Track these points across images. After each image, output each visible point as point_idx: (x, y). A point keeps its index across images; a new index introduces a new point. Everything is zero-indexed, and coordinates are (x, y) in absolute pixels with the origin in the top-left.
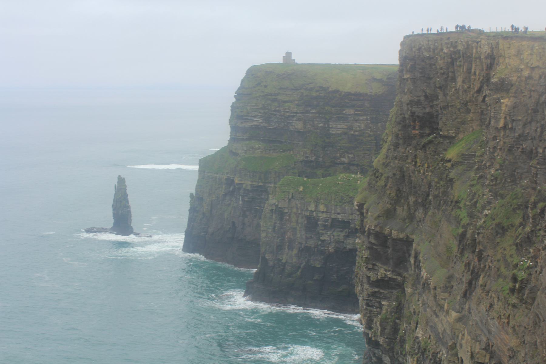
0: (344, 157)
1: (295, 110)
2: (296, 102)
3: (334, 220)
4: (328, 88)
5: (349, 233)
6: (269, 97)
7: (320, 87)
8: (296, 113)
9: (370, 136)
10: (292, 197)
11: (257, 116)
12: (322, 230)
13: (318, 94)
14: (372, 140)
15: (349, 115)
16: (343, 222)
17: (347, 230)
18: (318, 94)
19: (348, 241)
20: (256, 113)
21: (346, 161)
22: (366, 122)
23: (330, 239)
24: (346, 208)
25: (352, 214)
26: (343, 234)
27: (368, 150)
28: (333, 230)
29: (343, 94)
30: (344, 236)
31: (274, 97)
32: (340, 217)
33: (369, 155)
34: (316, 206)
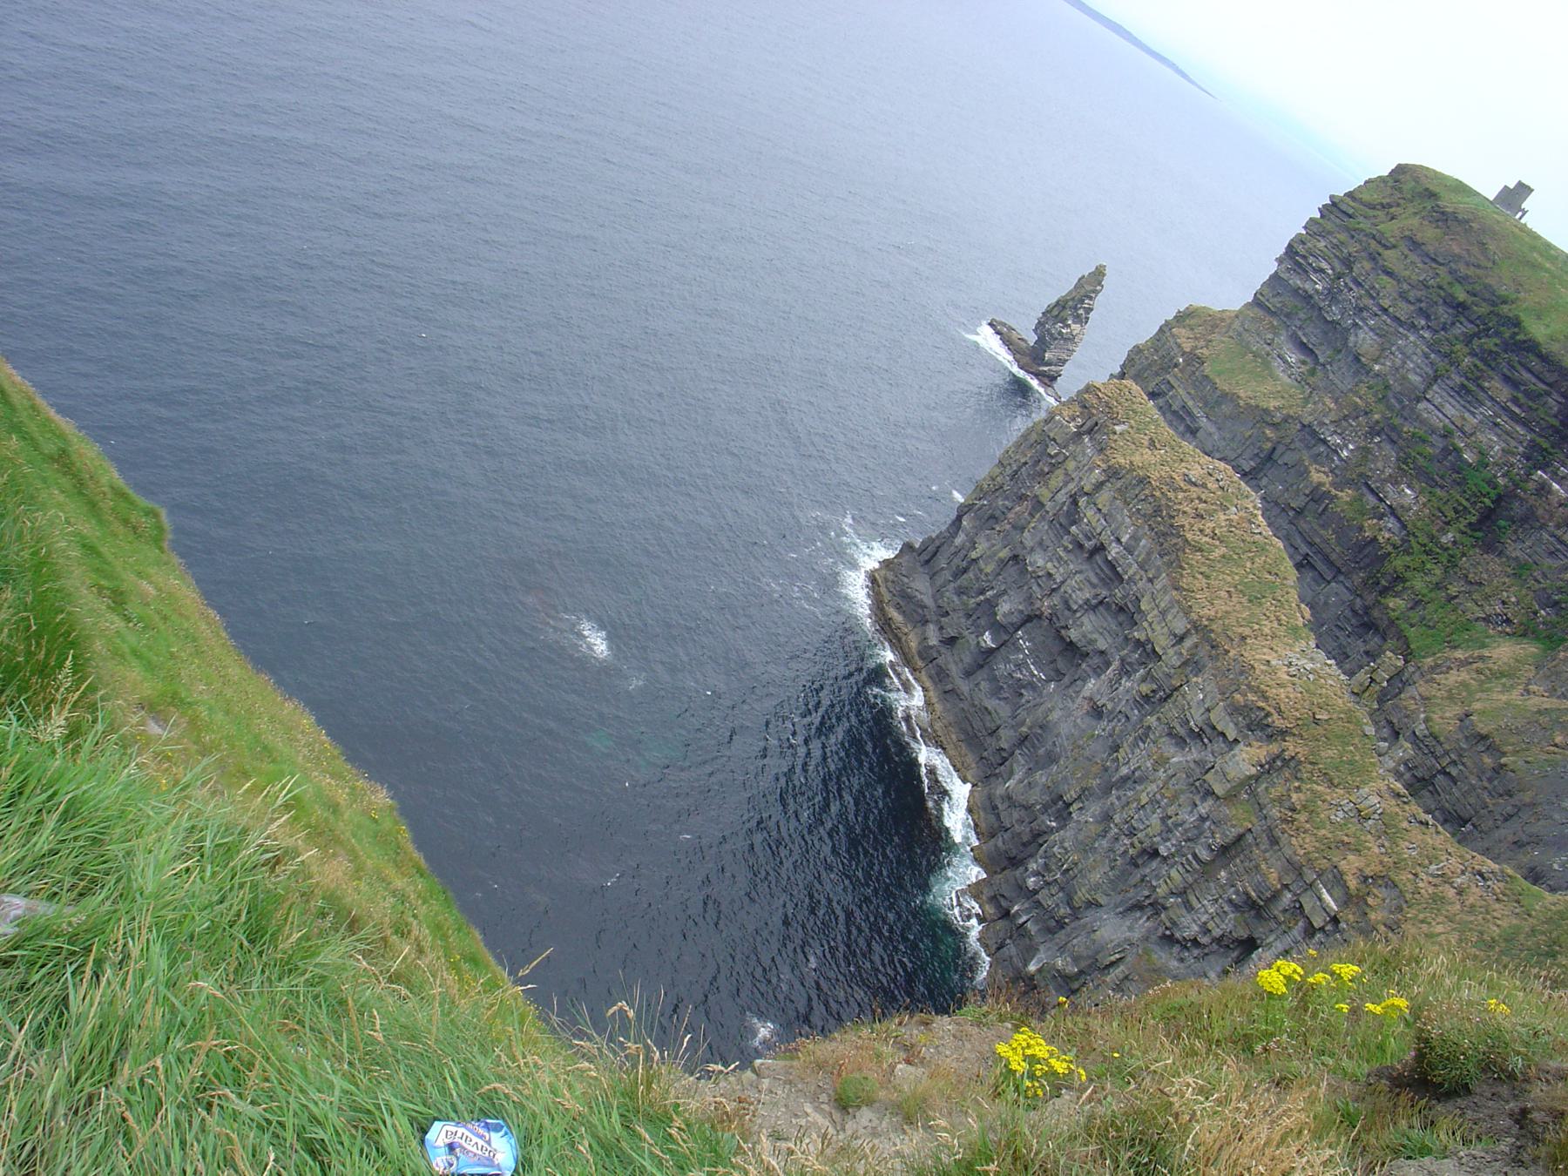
0: (1396, 483)
1: (1386, 303)
2: (1405, 286)
3: (1101, 548)
5: (1101, 602)
6: (1373, 244)
7: (1487, 287)
8: (1385, 310)
9: (1492, 483)
10: (1090, 431)
11: (1322, 271)
12: (1065, 548)
13: (1470, 300)
15: (1492, 399)
16: (1112, 566)
18: (1470, 300)
19: (1085, 620)
20: (1324, 265)
22: (1513, 443)
24: (1143, 542)
25: (1141, 566)
27: (1456, 512)
28: (1085, 567)
29: (1520, 337)
30: (1087, 602)
31: (1381, 250)
32: (1114, 551)
33: (1448, 523)
34: (1099, 486)
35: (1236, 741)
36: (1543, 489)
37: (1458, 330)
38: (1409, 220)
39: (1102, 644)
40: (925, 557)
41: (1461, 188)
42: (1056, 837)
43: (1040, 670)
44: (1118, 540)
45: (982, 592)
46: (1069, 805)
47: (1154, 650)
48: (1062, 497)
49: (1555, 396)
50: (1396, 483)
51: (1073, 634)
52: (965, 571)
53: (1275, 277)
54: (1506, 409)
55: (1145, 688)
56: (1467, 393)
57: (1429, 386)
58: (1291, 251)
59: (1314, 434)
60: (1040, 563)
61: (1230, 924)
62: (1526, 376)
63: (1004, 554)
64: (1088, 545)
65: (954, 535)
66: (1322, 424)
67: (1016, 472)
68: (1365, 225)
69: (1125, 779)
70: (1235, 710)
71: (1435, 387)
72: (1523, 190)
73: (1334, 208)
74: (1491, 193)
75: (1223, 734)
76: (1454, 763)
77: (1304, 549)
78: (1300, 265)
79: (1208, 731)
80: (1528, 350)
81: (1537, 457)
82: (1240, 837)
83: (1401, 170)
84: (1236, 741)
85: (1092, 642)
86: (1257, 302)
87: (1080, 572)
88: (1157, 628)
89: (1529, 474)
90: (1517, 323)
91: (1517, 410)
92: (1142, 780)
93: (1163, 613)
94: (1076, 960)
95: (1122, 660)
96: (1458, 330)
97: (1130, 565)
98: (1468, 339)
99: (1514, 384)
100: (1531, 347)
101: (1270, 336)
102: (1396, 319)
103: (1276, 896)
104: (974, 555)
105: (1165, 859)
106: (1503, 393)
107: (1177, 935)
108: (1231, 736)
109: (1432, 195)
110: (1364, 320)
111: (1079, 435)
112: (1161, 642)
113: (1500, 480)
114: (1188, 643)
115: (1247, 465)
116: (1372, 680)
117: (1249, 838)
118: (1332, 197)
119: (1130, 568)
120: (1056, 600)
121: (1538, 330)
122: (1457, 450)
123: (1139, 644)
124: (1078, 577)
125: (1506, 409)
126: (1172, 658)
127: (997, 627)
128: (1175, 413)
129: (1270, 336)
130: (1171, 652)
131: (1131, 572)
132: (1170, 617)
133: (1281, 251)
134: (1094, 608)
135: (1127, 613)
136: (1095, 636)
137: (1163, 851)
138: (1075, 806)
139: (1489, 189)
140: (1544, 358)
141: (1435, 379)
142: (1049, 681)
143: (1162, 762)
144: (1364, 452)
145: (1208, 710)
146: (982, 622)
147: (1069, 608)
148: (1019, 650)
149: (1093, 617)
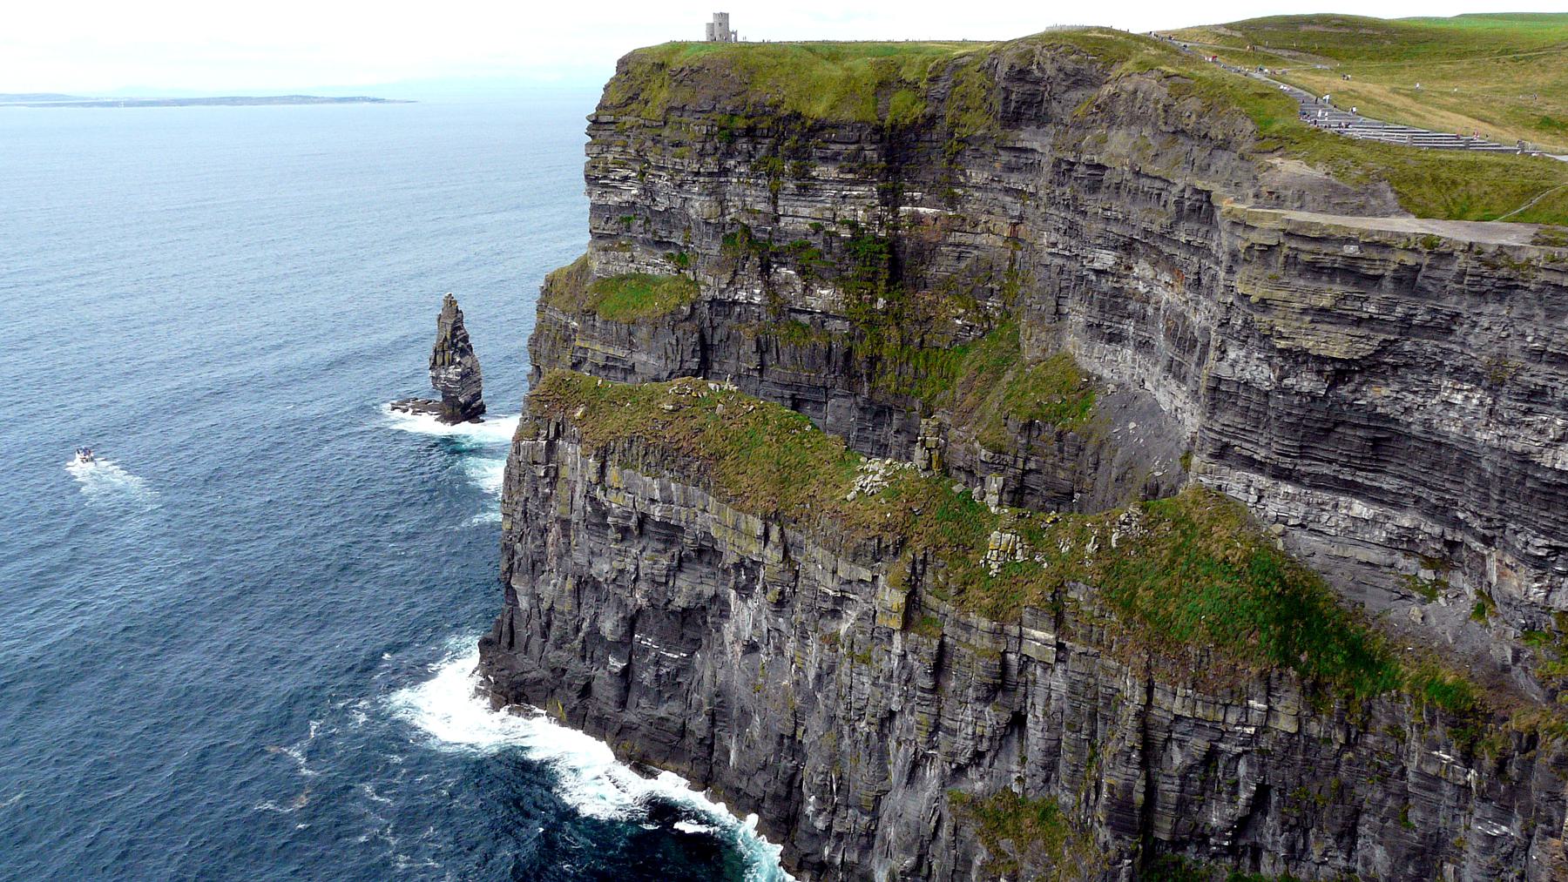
0: (812, 293)
1: (695, 167)
3: (643, 519)
4: (777, 106)
5: (681, 560)
8: (697, 174)
10: (558, 434)
14: (881, 252)
16: (663, 524)
17: (675, 550)
20: (625, 172)
22: (867, 202)
23: (637, 569)
25: (686, 505)
26: (664, 562)
27: (869, 280)
28: (644, 542)
29: (809, 123)
32: (656, 513)
34: (602, 471)
35: (875, 578)
36: (917, 220)
37: (763, 150)
38: (661, 95)
39: (709, 591)
40: (505, 641)
41: (675, 48)
42: (807, 771)
43: (677, 651)
44: (653, 501)
45: (578, 629)
46: (793, 737)
47: (753, 562)
48: (579, 502)
49: (867, 146)
50: (812, 293)
51: (680, 602)
52: (549, 624)
53: (595, 208)
54: (841, 181)
55: (772, 595)
56: (807, 188)
57: (775, 204)
58: (591, 180)
59: (722, 303)
60: (606, 567)
61: (993, 717)
62: (836, 147)
63: (570, 584)
64: (632, 523)
65: (515, 602)
66: (722, 291)
67: (525, 513)
68: (630, 120)
69: (819, 677)
70: (855, 557)
71: (780, 203)
72: (723, 18)
73: (596, 123)
74: (702, 36)
75: (861, 581)
76: (1026, 460)
77: (787, 393)
78: (606, 185)
79: (847, 587)
80: (822, 128)
81: (891, 198)
82: (942, 645)
83: (622, 63)
84: (875, 578)
85: (700, 595)
86: (597, 236)
87: (644, 549)
88: (744, 543)
89: (896, 215)
90: (797, 116)
91: (850, 176)
92: (832, 669)
93: (736, 528)
94: (907, 850)
95: (736, 588)
96: (763, 150)
97: (678, 512)
98: (774, 151)
99: (833, 159)
100: (819, 127)
101: (628, 255)
102: (711, 174)
103: (1005, 665)
104: (545, 606)
105: (902, 711)
106: (831, 171)
107: (962, 760)
108: (866, 575)
109: (662, 66)
110: (688, 191)
111: (551, 447)
112: (755, 549)
113: (882, 234)
114: (774, 535)
115: (693, 364)
116: (930, 450)
117: (947, 639)
118: (588, 118)
119: (680, 515)
120: (643, 586)
121: (818, 109)
122: (835, 234)
123: (738, 566)
124: (648, 553)
125: (841, 181)
126: (773, 555)
127: (618, 647)
128: (604, 367)
129: (628, 255)
130: (768, 552)
131: (683, 517)
132: (743, 526)
133: (583, 184)
134: (680, 568)
135: (706, 552)
136: (698, 589)
137: (895, 707)
138: (800, 733)
139: (695, 31)
140: (835, 126)
141: (775, 196)
142: (691, 654)
143: (832, 641)
144: (770, 288)
145: (834, 572)
146: (598, 653)
147: (660, 584)
148: (646, 650)
149: (682, 576)
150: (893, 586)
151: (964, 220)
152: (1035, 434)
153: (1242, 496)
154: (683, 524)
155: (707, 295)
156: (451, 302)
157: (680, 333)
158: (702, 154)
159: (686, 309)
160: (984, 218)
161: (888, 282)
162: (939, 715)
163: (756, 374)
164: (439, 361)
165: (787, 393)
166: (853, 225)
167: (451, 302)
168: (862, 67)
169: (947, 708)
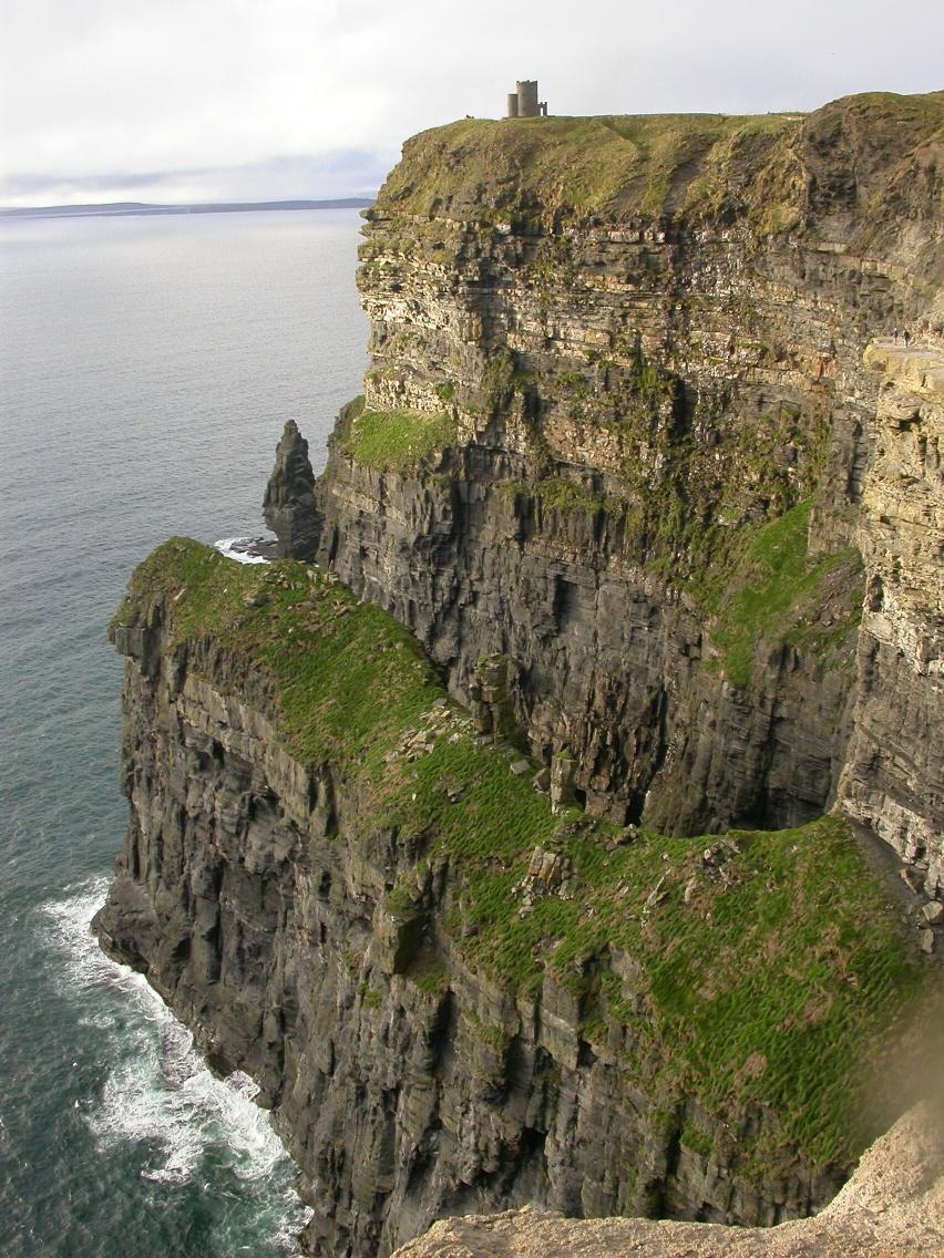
21: (588, 455)
44: (224, 726)
56: (582, 303)
57: (543, 322)
64: (208, 749)
66: (480, 435)
71: (549, 323)
72: (529, 88)
91: (630, 287)
102: (471, 283)
113: (671, 367)
122: (614, 365)
128: (358, 523)
136: (269, 848)
150: (388, 909)
151: (765, 351)
152: (790, 666)
153: (895, 843)
154: (252, 761)
155: (463, 440)
156: (291, 427)
157: (429, 487)
158: (461, 260)
159: (438, 455)
160: (789, 348)
161: (670, 433)
162: (437, 1106)
163: (515, 545)
164: (273, 497)
165: (552, 573)
166: (636, 354)
167: (291, 427)
168: (663, 146)
169: (447, 1099)
